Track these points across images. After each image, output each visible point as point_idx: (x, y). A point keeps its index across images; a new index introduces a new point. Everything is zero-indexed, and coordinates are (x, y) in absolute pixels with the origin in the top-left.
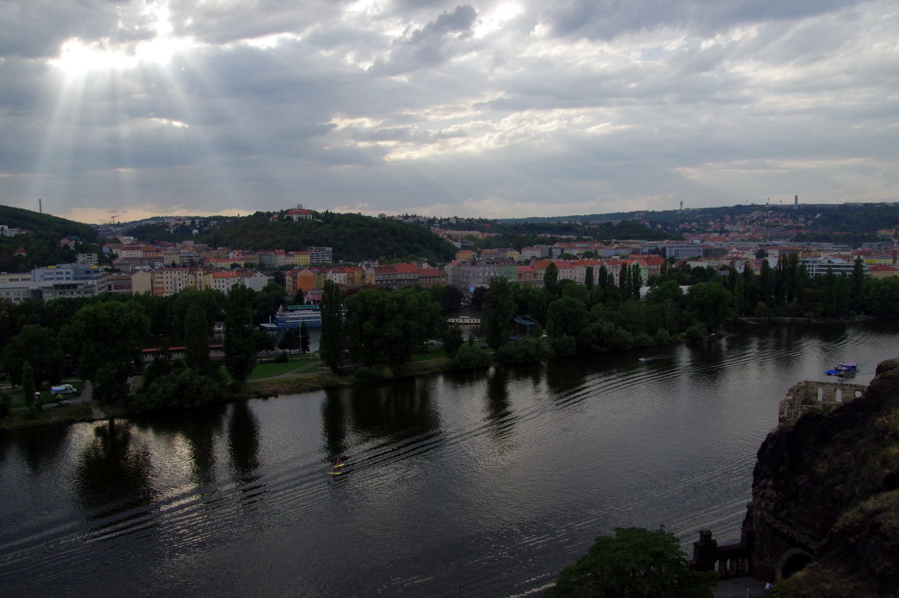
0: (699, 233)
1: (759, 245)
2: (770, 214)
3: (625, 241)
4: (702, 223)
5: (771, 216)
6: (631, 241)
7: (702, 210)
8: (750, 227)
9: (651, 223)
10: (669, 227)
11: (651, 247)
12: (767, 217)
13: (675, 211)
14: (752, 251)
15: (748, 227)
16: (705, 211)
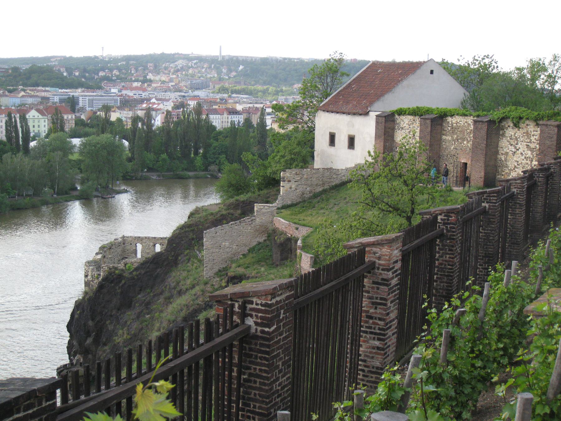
0: (120, 82)
1: (179, 96)
2: (195, 64)
3: (35, 88)
4: (124, 71)
5: (195, 66)
6: (40, 88)
7: (124, 56)
8: (174, 76)
9: (67, 70)
10: (87, 75)
11: (62, 95)
12: (192, 67)
13: (96, 57)
14: (172, 102)
15: (171, 77)
16: (128, 59)
